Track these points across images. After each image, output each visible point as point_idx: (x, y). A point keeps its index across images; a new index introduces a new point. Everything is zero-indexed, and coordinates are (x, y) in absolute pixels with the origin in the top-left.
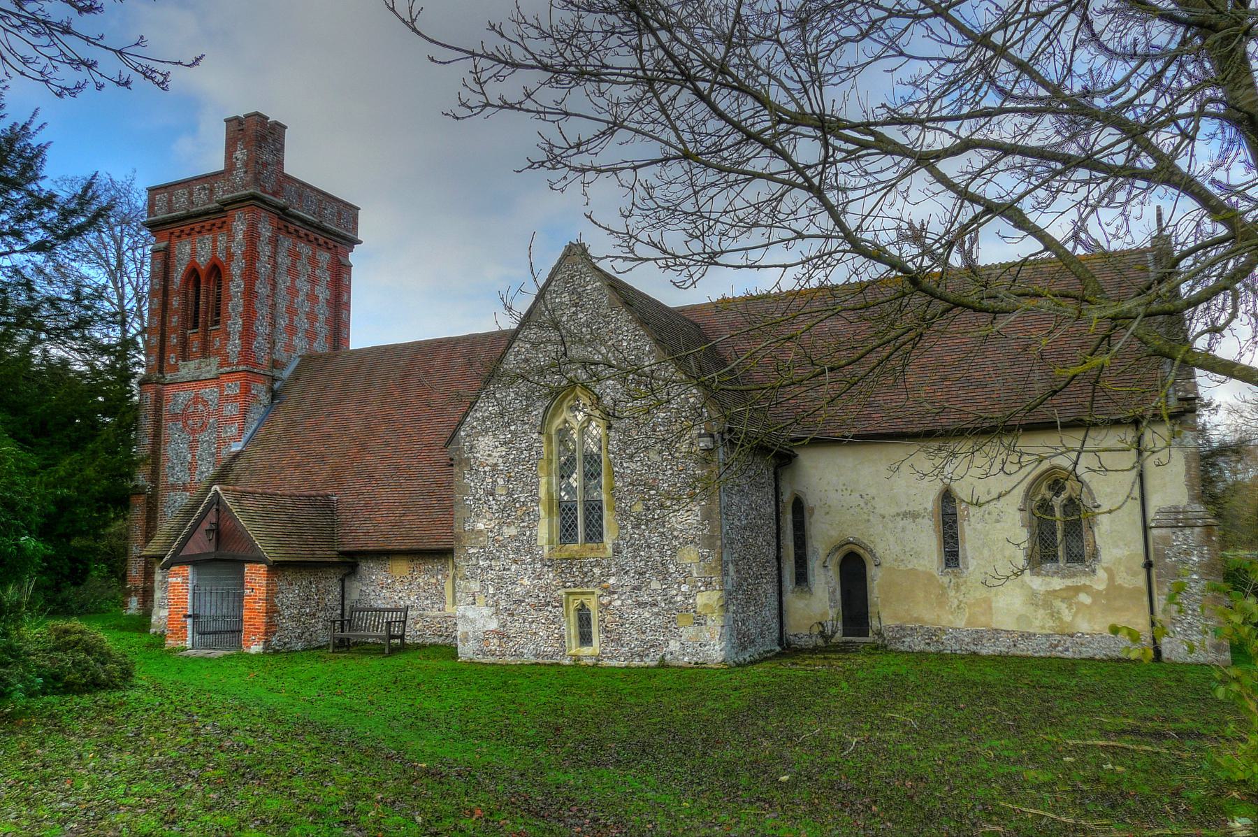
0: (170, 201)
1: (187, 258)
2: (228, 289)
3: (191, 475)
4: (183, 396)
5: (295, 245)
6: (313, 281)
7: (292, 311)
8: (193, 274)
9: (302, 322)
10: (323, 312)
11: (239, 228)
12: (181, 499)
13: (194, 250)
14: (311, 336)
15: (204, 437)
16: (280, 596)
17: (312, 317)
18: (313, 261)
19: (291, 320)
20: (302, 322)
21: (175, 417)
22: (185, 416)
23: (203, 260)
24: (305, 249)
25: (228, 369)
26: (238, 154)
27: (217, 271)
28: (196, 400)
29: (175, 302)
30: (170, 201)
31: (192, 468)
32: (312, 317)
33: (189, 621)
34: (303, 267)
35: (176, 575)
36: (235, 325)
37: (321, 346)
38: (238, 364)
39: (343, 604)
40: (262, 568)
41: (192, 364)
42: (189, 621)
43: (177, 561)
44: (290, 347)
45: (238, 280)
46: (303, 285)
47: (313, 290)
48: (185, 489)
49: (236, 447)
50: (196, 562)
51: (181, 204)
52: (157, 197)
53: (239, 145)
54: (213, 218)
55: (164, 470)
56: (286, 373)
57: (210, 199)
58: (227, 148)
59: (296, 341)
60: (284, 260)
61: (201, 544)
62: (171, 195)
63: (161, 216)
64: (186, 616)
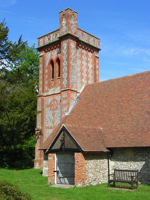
0: (44, 41)
1: (49, 57)
2: (62, 65)
3: (53, 124)
4: (50, 99)
5: (81, 50)
6: (87, 62)
7: (82, 71)
8: (52, 62)
9: (85, 75)
10: (91, 72)
11: (64, 44)
12: (50, 131)
13: (51, 55)
14: (88, 79)
15: (57, 111)
16: (88, 164)
17: (87, 73)
18: (87, 56)
19: (82, 74)
20: (85, 75)
21: (48, 106)
22: (51, 105)
23: (54, 58)
24: (84, 51)
25: (64, 89)
26: (64, 22)
27: (58, 60)
28: (54, 100)
29: (46, 71)
30: (44, 41)
31: (53, 122)
32: (87, 73)
33: (56, 173)
34: (84, 57)
35: (51, 156)
36: (65, 75)
37: (91, 82)
38: (66, 87)
39: (109, 168)
40: (80, 154)
41: (52, 89)
42: (56, 173)
43: (51, 151)
44: (82, 83)
45: (65, 61)
46: (84, 63)
47: (87, 65)
48: (51, 128)
49: (67, 114)
50: (56, 151)
51: (47, 41)
52: (40, 40)
53: (64, 19)
54: (57, 45)
55: (45, 122)
56: (81, 91)
57: (55, 38)
58: (60, 21)
59: (83, 80)
60: (78, 55)
61: (57, 146)
62: (44, 39)
63: (42, 45)
64: (54, 171)
